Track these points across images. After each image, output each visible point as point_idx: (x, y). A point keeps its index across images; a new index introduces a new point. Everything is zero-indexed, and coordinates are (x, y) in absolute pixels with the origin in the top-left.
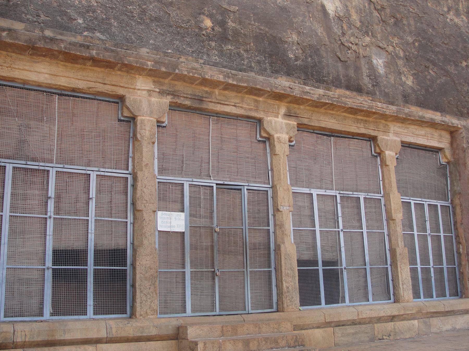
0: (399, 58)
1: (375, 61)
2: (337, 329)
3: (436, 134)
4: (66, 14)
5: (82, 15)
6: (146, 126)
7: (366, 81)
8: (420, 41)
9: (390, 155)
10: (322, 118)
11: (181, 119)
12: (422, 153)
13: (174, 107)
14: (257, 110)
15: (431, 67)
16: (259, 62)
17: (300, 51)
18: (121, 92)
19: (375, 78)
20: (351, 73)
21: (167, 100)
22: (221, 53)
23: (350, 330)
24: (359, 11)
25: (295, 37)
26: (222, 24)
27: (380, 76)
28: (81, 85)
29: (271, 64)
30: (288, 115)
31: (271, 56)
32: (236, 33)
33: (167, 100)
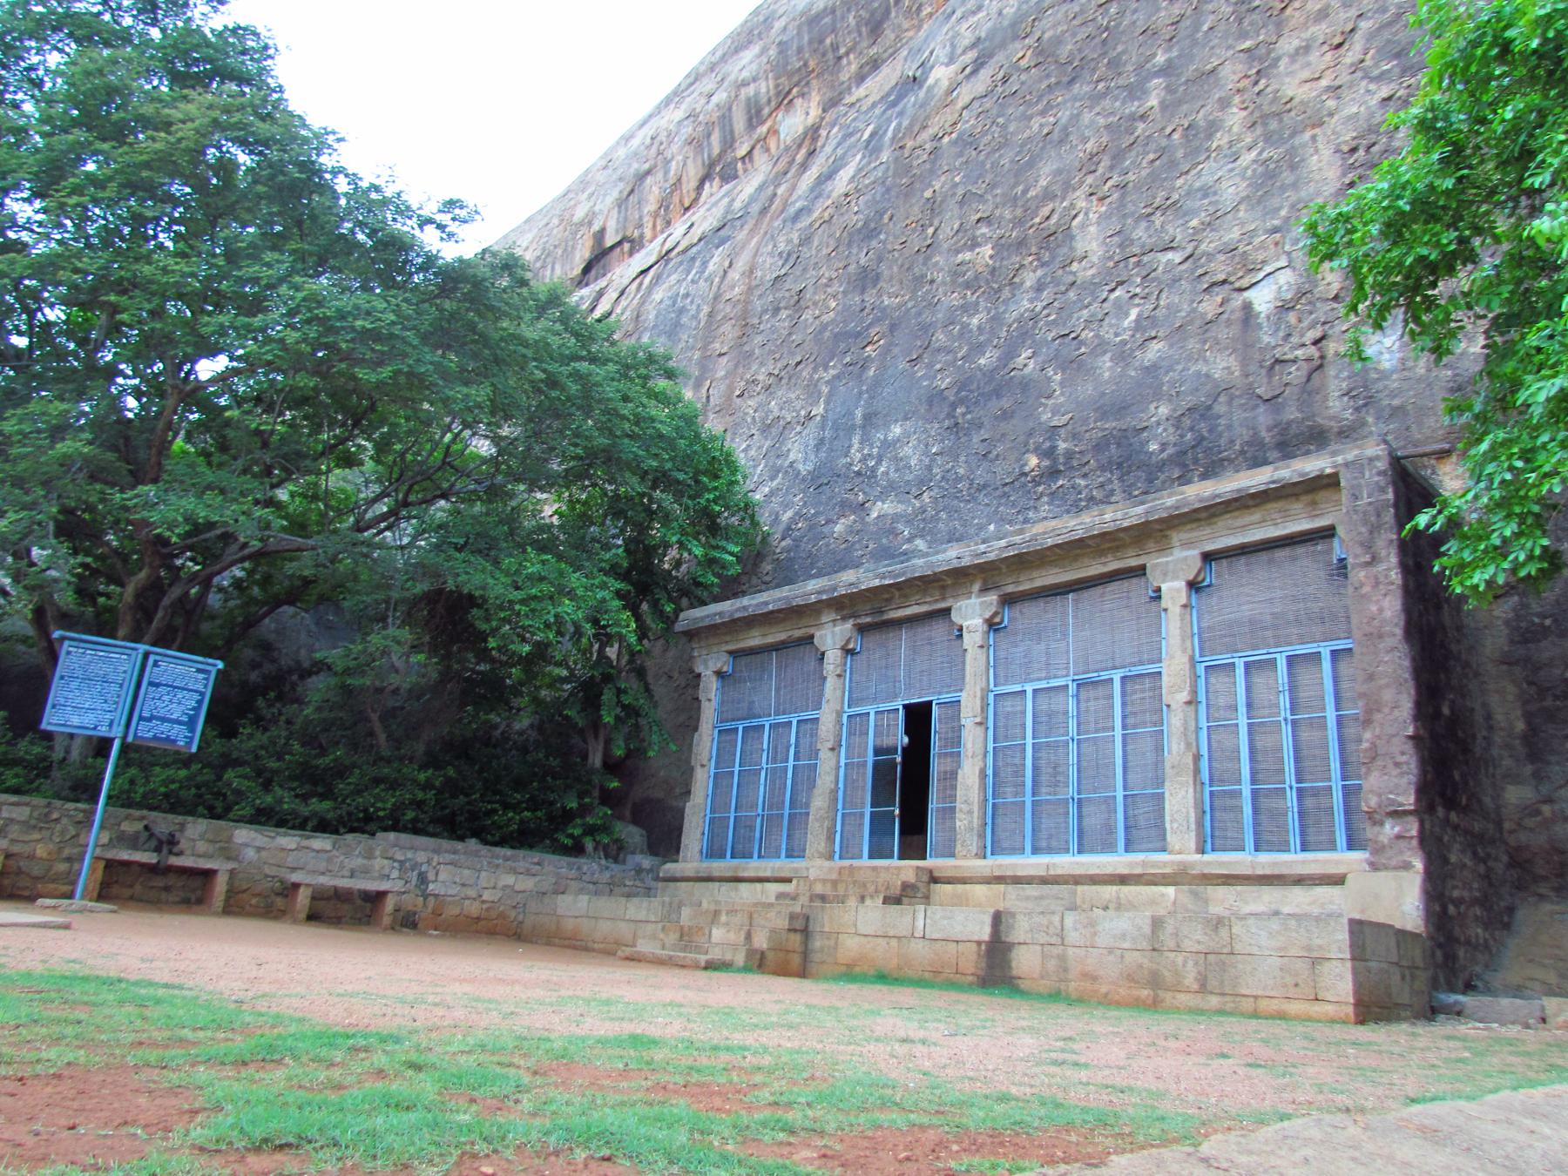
2: (1010, 887)
3: (1297, 506)
7: (1336, 406)
10: (1035, 574)
11: (874, 639)
12: (1280, 554)
14: (944, 599)
16: (1102, 486)
17: (1171, 430)
19: (1365, 387)
20: (1292, 413)
21: (849, 625)
23: (1032, 890)
26: (1050, 453)
27: (1384, 375)
28: (782, 636)
29: (1121, 479)
30: (985, 590)
32: (1069, 455)
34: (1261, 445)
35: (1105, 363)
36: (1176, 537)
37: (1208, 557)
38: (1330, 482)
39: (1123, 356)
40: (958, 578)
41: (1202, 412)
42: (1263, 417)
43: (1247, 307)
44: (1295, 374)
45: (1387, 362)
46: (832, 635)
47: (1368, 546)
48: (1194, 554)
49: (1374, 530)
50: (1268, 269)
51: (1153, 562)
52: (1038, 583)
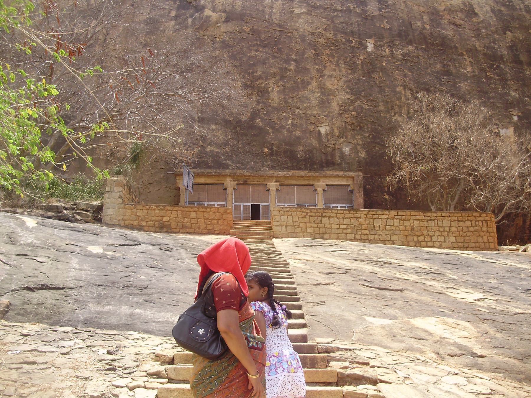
0: (358, 144)
1: (344, 150)
3: (345, 179)
4: (218, 156)
5: (223, 155)
6: (230, 190)
8: (373, 135)
9: (320, 190)
15: (377, 146)
16: (285, 161)
18: (223, 182)
20: (329, 158)
21: (236, 183)
22: (271, 160)
24: (339, 128)
25: (302, 148)
26: (271, 149)
27: (346, 155)
28: (212, 182)
30: (276, 182)
31: (290, 158)
32: (277, 152)
33: (236, 183)
35: (285, 131)
36: (321, 180)
37: (327, 185)
39: (289, 131)
41: (310, 151)
43: (319, 131)
44: (330, 149)
45: (347, 153)
47: (359, 190)
49: (360, 187)
50: (324, 125)
52: (290, 183)
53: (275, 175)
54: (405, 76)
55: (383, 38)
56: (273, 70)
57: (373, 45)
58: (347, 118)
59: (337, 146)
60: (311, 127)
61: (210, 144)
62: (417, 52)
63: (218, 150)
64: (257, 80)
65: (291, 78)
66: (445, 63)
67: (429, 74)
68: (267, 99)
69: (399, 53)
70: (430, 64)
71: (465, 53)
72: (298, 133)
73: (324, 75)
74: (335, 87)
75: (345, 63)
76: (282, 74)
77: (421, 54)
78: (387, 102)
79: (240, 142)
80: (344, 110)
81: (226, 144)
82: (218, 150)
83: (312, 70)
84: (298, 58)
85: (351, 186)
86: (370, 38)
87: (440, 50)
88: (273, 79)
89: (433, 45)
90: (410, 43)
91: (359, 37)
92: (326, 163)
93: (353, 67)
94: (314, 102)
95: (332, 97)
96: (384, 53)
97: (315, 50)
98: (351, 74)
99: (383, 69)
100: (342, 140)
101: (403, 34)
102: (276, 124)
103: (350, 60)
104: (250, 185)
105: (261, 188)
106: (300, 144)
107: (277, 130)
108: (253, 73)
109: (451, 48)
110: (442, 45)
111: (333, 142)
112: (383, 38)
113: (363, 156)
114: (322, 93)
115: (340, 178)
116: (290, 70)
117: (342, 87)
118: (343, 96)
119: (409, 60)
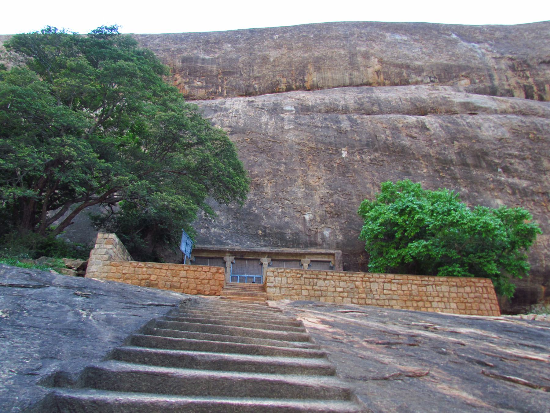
1: (325, 233)
3: (327, 257)
5: (225, 236)
7: (319, 240)
11: (238, 261)
12: (322, 263)
13: (235, 259)
20: (312, 239)
21: (234, 257)
22: (264, 240)
24: (320, 216)
25: (290, 231)
26: (265, 232)
27: (326, 238)
28: (213, 256)
30: (268, 257)
32: (269, 233)
33: (234, 257)
34: (307, 243)
35: (276, 218)
36: (307, 257)
37: (311, 261)
38: (333, 255)
39: (279, 218)
40: (264, 254)
41: (297, 234)
42: (308, 238)
43: (304, 218)
44: (313, 233)
45: (327, 236)
46: (229, 259)
47: (339, 265)
48: (309, 260)
49: (340, 263)
51: (302, 260)
53: (268, 251)
54: (373, 176)
55: (354, 147)
56: (268, 170)
57: (346, 153)
58: (327, 208)
59: (319, 230)
60: (298, 215)
61: (214, 227)
62: (382, 158)
63: (221, 232)
64: (254, 178)
65: (281, 176)
66: (405, 165)
67: (392, 174)
68: (262, 193)
69: (367, 158)
70: (393, 167)
71: (421, 158)
72: (287, 219)
73: (308, 175)
74: (317, 184)
75: (324, 166)
76: (275, 173)
77: (385, 158)
78: (359, 196)
79: (239, 225)
80: (324, 201)
81: (228, 227)
82: (221, 232)
83: (298, 171)
84: (287, 161)
85: (333, 262)
86: (344, 147)
87: (400, 156)
88: (268, 177)
89: (394, 152)
90: (376, 150)
91: (335, 146)
92: (310, 244)
93: (330, 169)
94: (300, 195)
95: (314, 192)
96: (355, 158)
97: (301, 155)
98: (329, 174)
99: (355, 171)
100: (323, 225)
101: (370, 144)
102: (269, 211)
103: (329, 164)
104: (245, 259)
105: (255, 263)
106: (289, 228)
107: (269, 216)
108: (251, 172)
109: (410, 154)
110: (402, 152)
111: (315, 227)
112: (354, 147)
113: (340, 238)
114: (306, 188)
115: (323, 256)
116: (280, 171)
117: (322, 184)
118: (323, 191)
119: (375, 164)
